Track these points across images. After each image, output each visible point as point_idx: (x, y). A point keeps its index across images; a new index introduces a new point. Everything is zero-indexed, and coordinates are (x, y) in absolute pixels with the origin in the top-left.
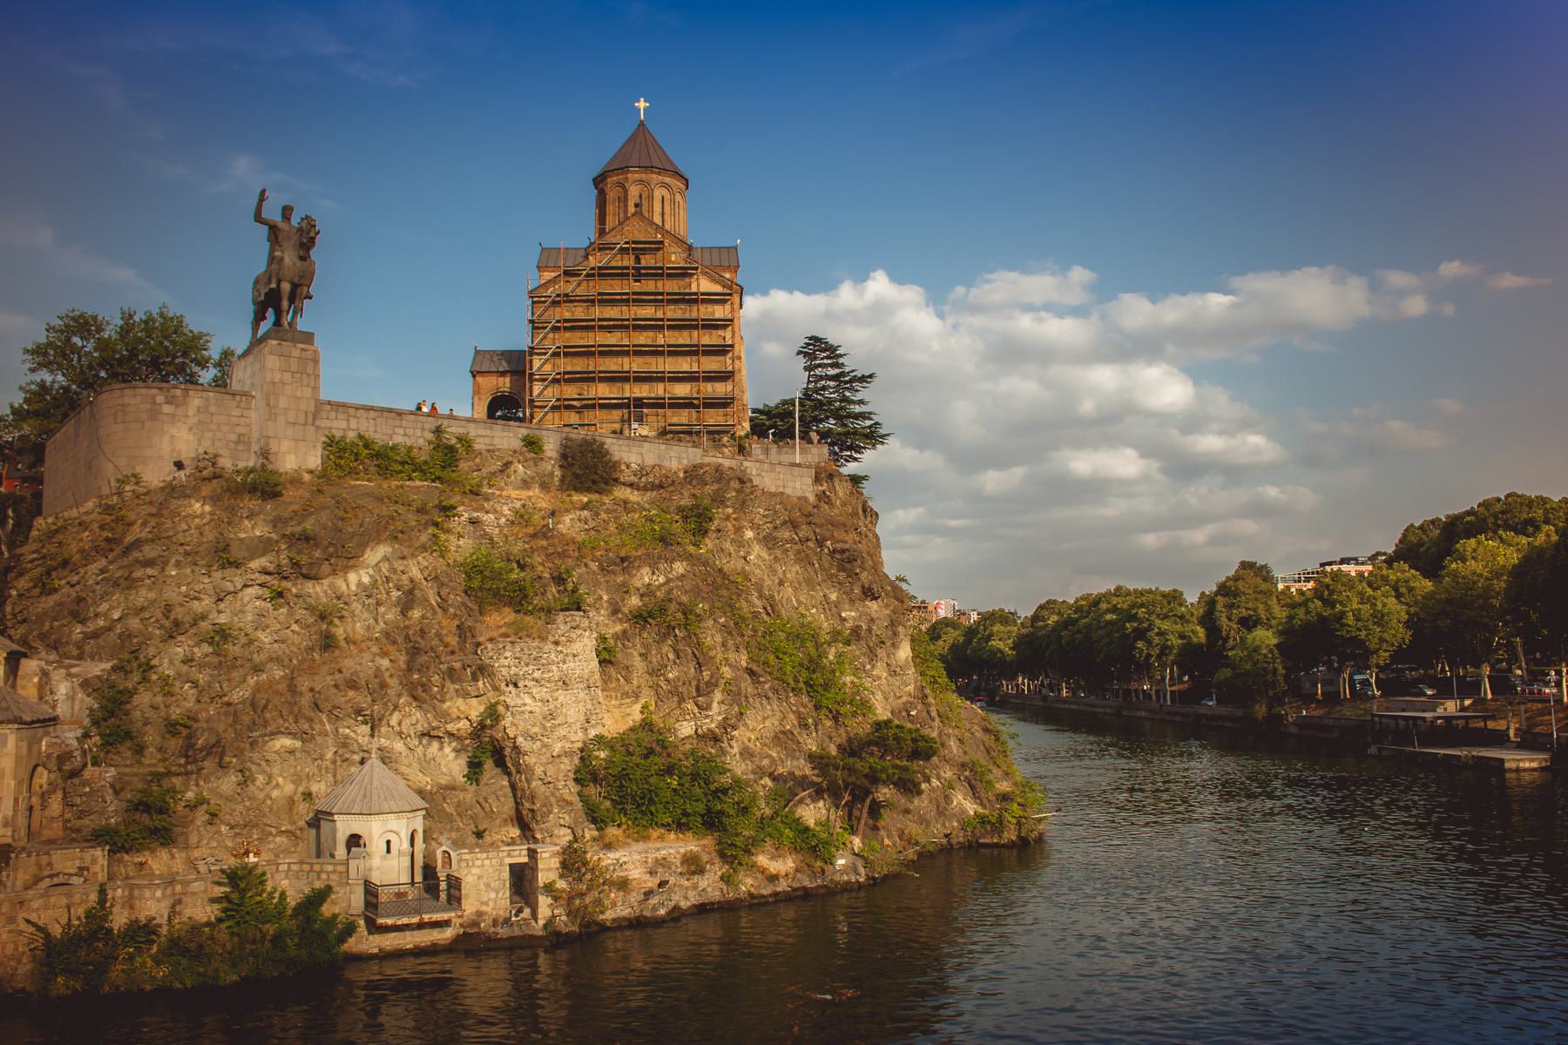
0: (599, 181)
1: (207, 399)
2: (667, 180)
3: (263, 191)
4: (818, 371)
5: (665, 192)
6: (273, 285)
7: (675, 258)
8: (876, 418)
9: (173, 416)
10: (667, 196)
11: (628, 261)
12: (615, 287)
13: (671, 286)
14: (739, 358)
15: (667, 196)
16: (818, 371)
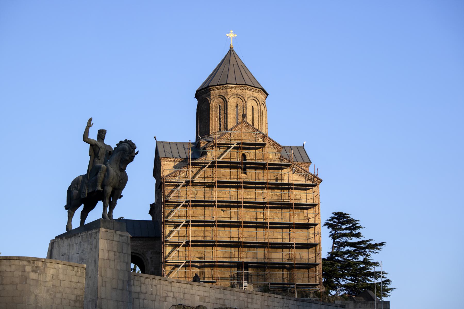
0: (202, 95)
1: (58, 270)
2: (256, 94)
3: (90, 120)
4: (344, 239)
5: (254, 104)
6: (99, 188)
7: (272, 156)
8: (387, 277)
9: (37, 281)
10: (256, 108)
11: (236, 157)
12: (224, 174)
13: (268, 176)
14: (319, 234)
15: (256, 108)
16: (344, 239)
